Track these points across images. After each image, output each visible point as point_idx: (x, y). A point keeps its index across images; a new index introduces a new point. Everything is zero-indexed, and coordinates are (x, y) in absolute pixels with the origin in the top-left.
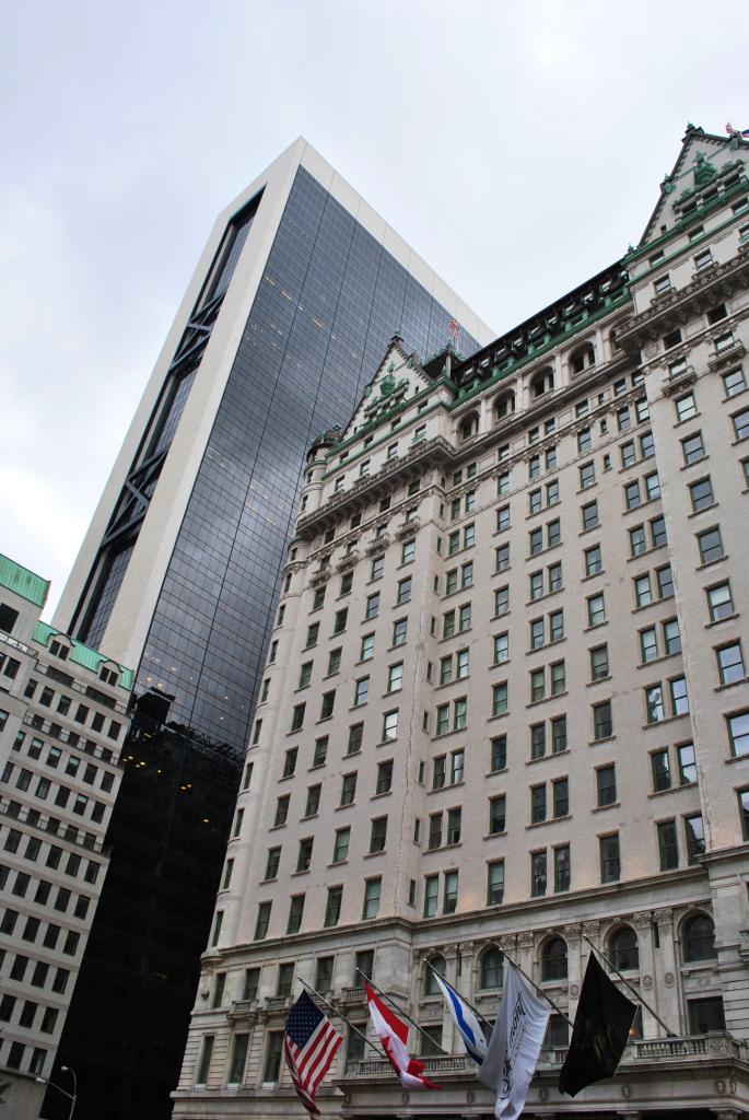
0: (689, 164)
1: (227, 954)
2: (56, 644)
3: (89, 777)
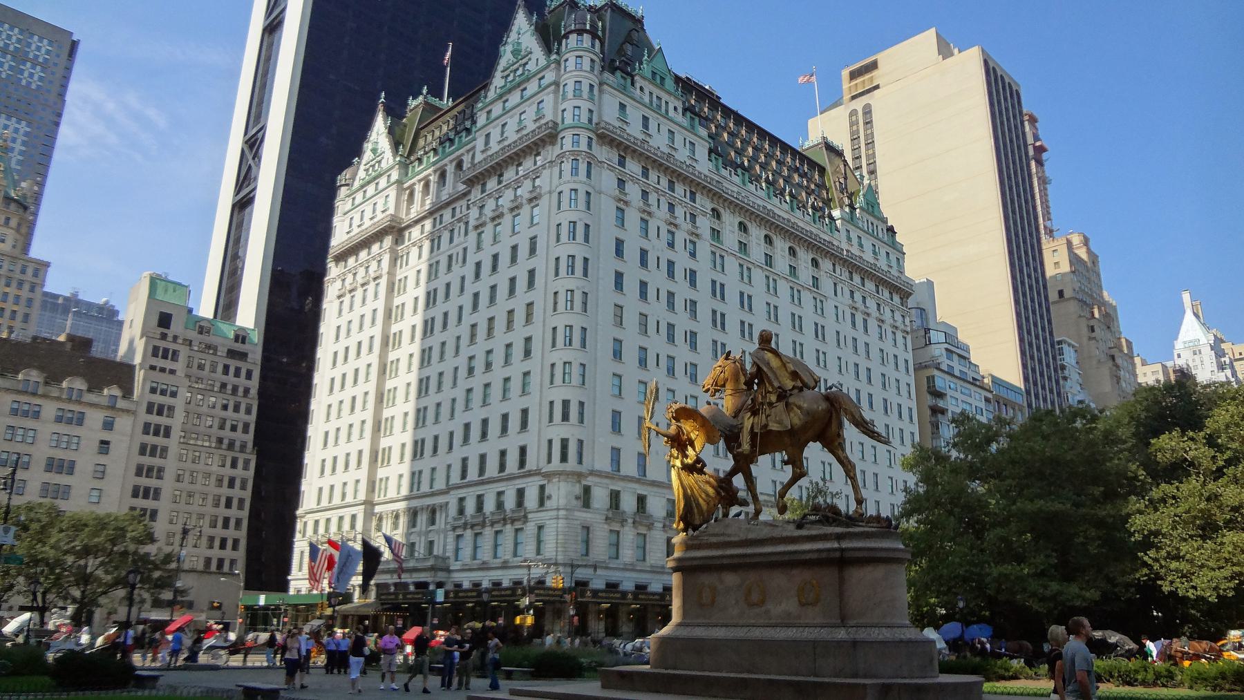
2: (202, 328)
3: (237, 408)
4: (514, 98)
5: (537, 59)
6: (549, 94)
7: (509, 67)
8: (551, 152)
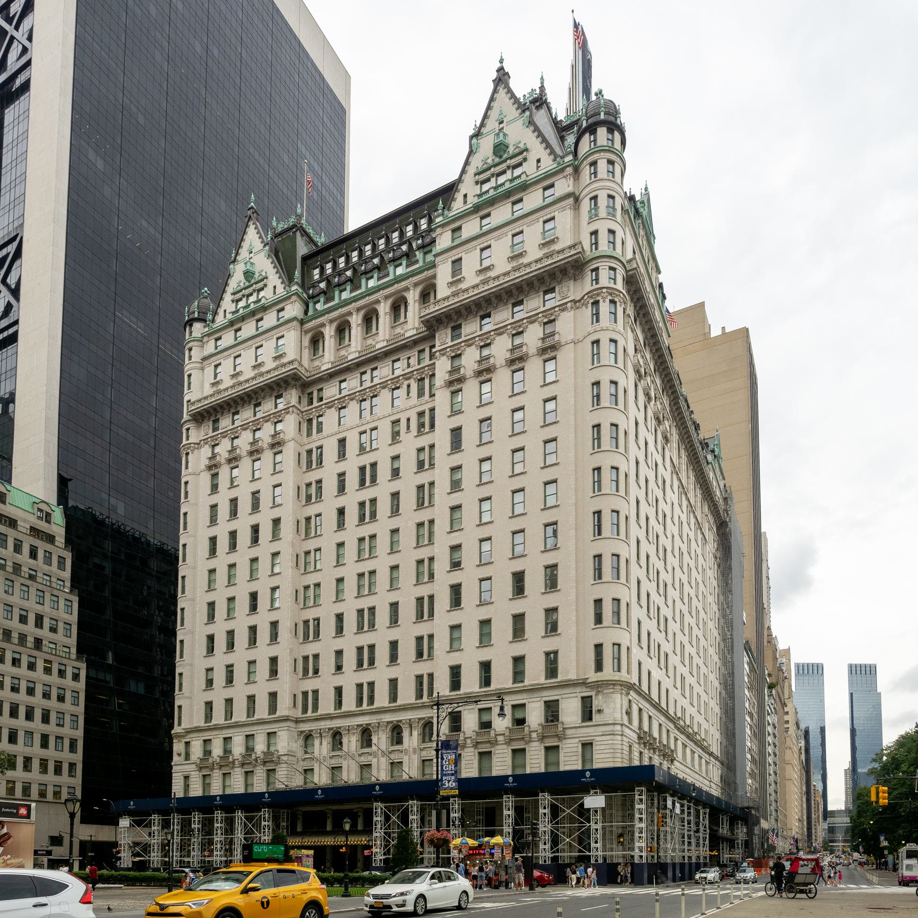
1: (189, 731)
6: (564, 209)
7: (489, 169)
8: (574, 290)
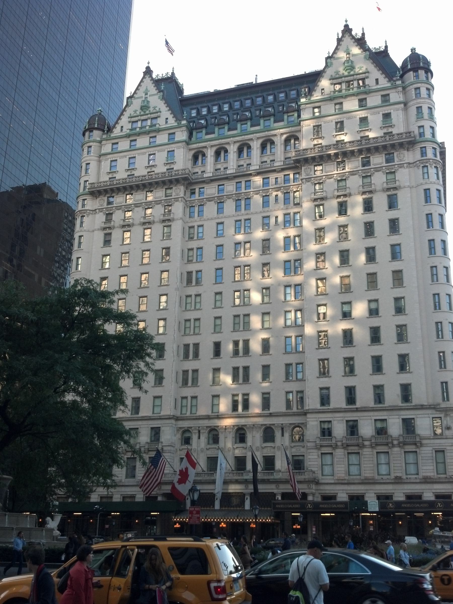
0: (141, 93)
4: (142, 141)
5: (167, 119)
